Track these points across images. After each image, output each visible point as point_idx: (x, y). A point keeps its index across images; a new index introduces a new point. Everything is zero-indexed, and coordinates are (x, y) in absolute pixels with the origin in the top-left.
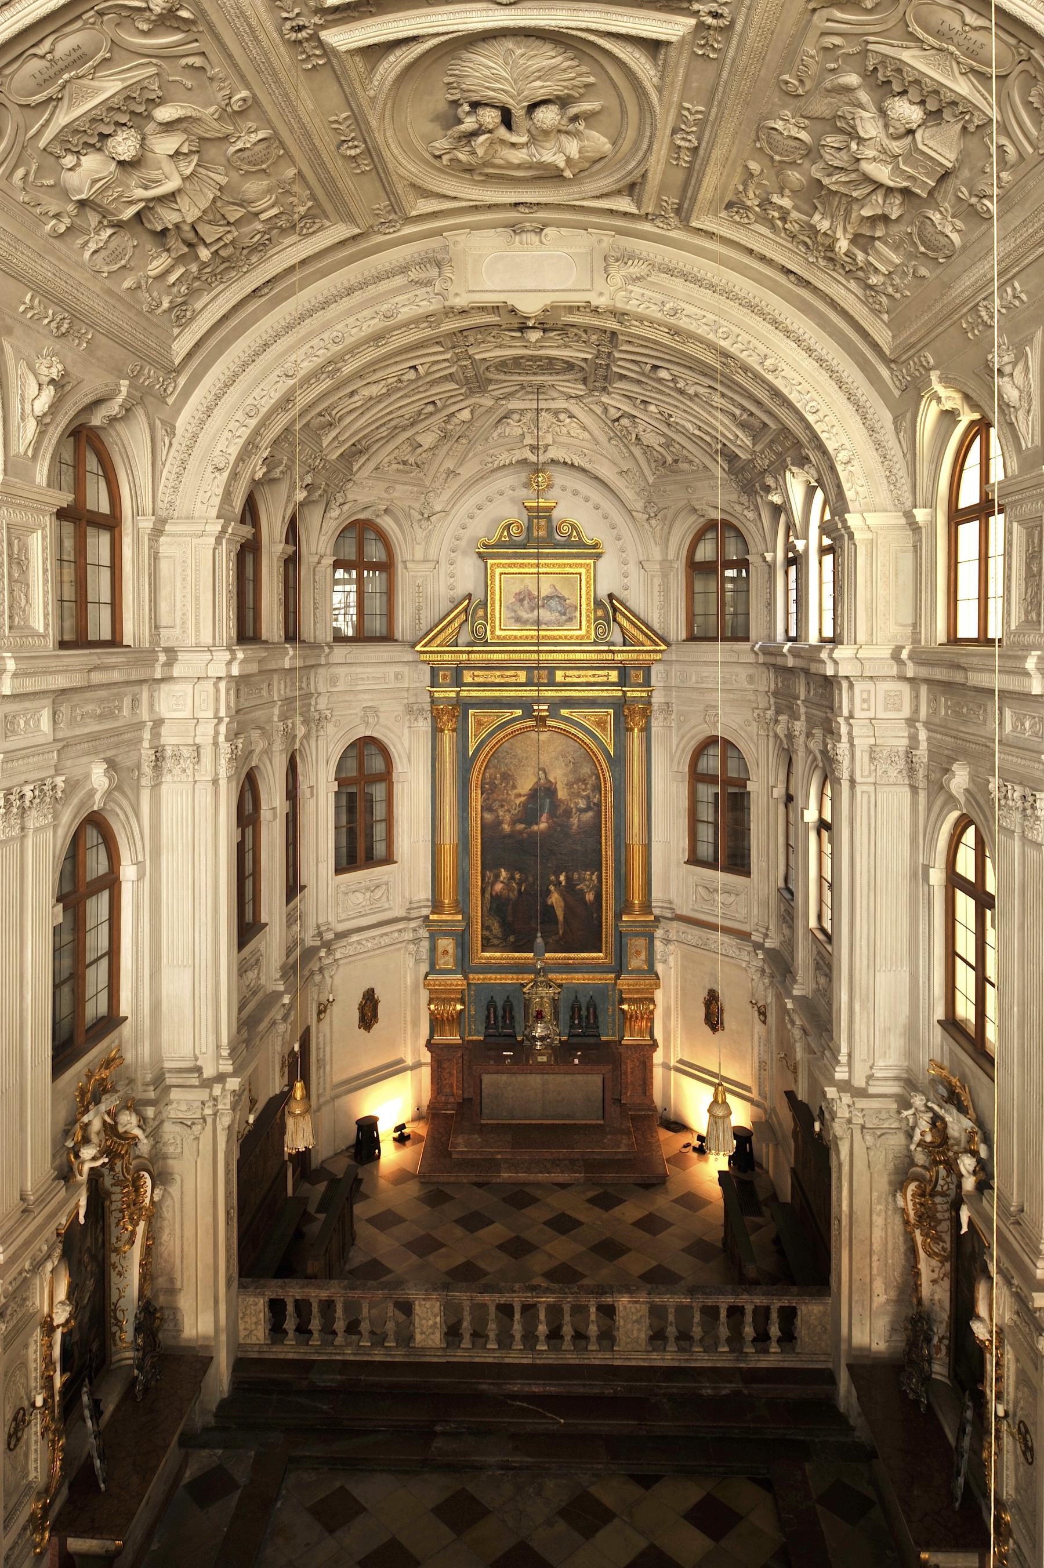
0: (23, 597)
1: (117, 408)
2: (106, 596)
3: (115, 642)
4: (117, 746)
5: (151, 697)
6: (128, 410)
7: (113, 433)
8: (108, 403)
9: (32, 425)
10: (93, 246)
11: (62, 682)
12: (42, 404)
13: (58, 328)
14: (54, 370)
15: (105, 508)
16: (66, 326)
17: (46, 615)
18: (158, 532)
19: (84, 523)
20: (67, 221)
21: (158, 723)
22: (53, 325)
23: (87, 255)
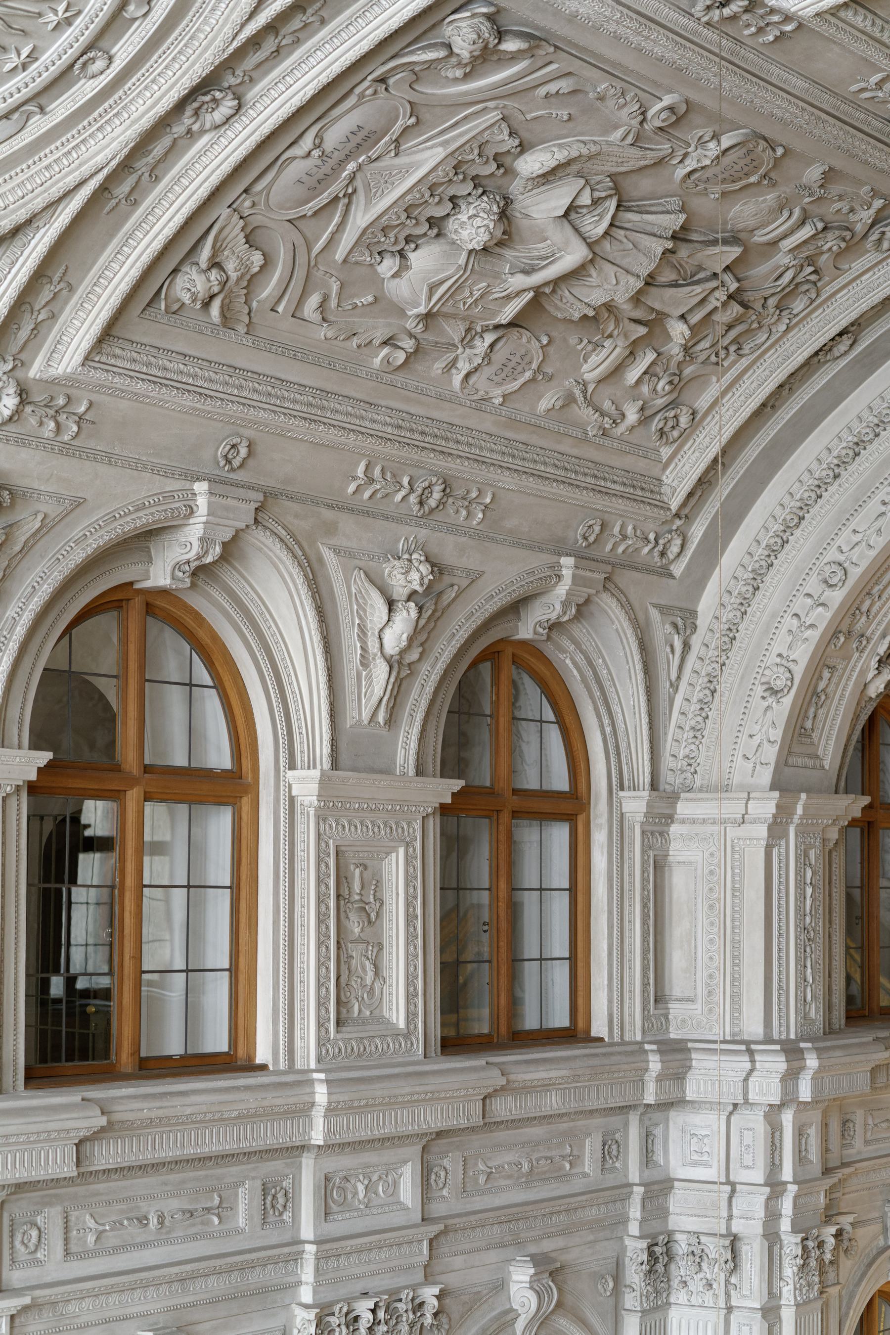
0: (369, 967)
1: (558, 607)
2: (559, 946)
3: (574, 1034)
4: (565, 1232)
5: (648, 1137)
6: (582, 609)
7: (566, 643)
8: (544, 599)
9: (380, 671)
10: (464, 367)
11: (431, 1119)
12: (396, 635)
13: (421, 503)
14: (415, 576)
15: (560, 781)
16: (437, 495)
17: (410, 997)
18: (660, 820)
19: (505, 816)
20: (408, 344)
21: (659, 1189)
22: (413, 499)
23: (457, 379)
